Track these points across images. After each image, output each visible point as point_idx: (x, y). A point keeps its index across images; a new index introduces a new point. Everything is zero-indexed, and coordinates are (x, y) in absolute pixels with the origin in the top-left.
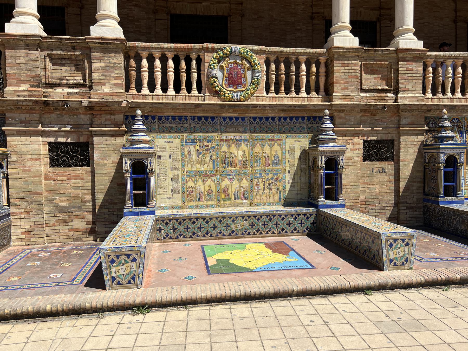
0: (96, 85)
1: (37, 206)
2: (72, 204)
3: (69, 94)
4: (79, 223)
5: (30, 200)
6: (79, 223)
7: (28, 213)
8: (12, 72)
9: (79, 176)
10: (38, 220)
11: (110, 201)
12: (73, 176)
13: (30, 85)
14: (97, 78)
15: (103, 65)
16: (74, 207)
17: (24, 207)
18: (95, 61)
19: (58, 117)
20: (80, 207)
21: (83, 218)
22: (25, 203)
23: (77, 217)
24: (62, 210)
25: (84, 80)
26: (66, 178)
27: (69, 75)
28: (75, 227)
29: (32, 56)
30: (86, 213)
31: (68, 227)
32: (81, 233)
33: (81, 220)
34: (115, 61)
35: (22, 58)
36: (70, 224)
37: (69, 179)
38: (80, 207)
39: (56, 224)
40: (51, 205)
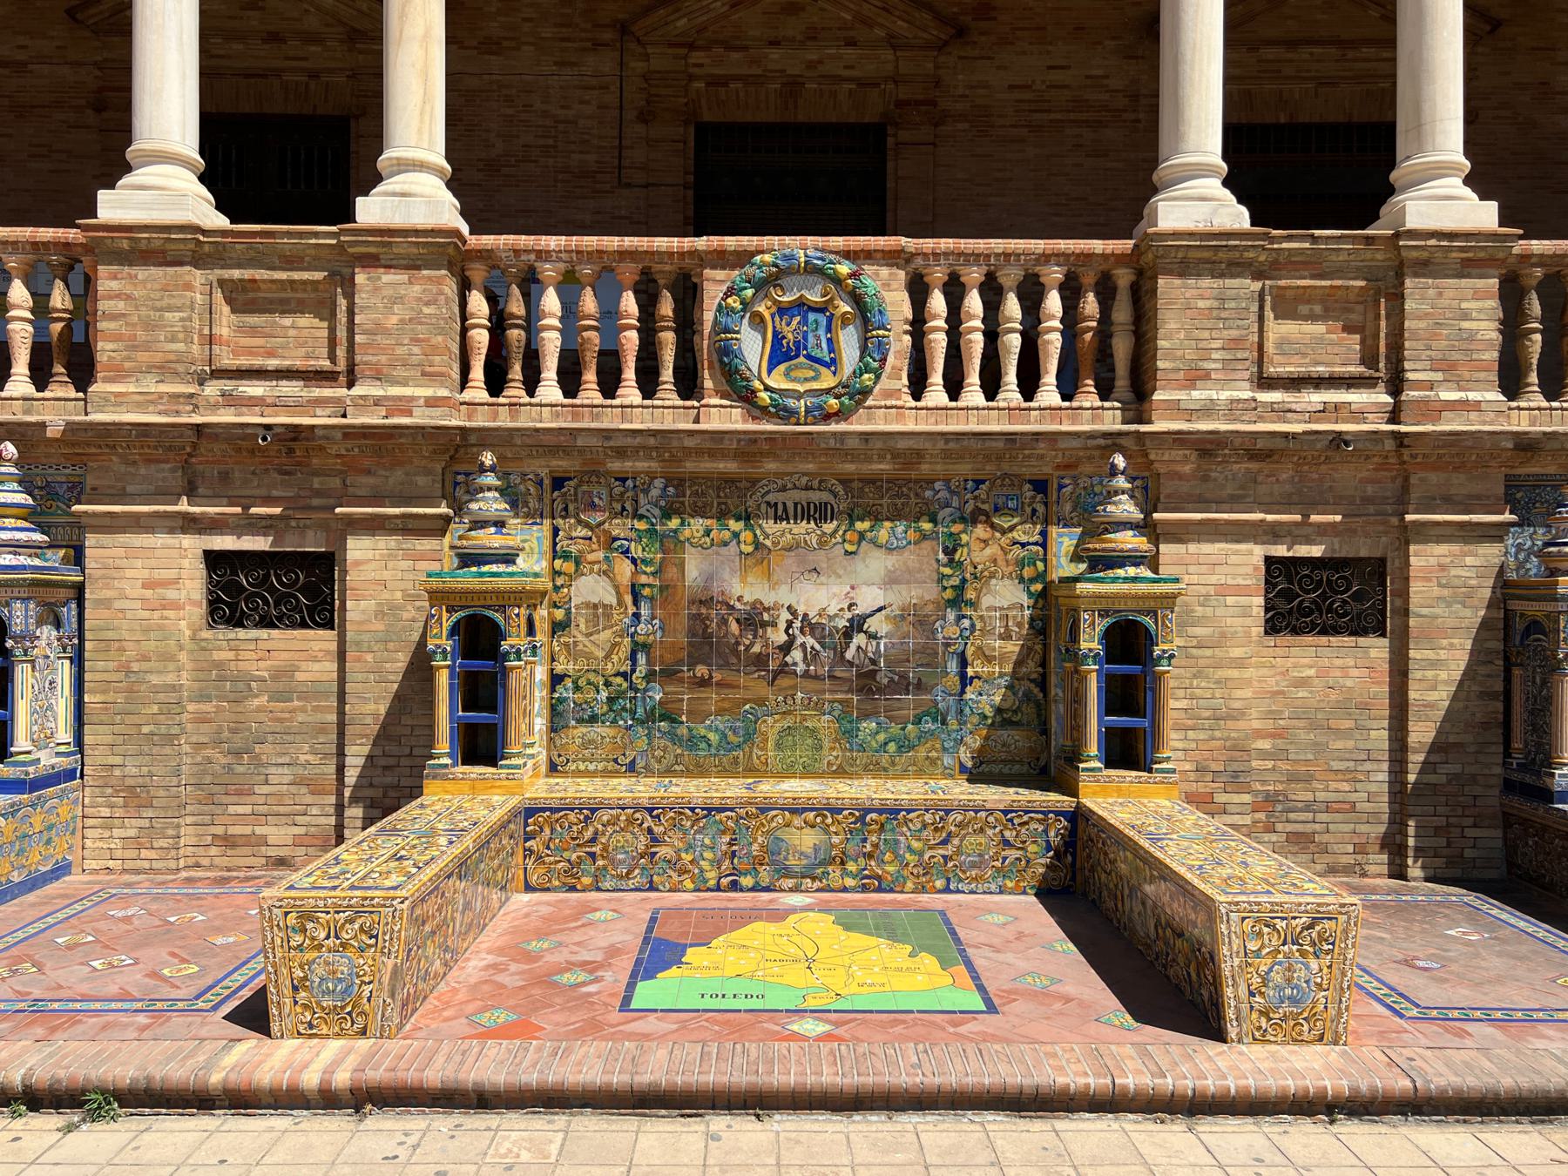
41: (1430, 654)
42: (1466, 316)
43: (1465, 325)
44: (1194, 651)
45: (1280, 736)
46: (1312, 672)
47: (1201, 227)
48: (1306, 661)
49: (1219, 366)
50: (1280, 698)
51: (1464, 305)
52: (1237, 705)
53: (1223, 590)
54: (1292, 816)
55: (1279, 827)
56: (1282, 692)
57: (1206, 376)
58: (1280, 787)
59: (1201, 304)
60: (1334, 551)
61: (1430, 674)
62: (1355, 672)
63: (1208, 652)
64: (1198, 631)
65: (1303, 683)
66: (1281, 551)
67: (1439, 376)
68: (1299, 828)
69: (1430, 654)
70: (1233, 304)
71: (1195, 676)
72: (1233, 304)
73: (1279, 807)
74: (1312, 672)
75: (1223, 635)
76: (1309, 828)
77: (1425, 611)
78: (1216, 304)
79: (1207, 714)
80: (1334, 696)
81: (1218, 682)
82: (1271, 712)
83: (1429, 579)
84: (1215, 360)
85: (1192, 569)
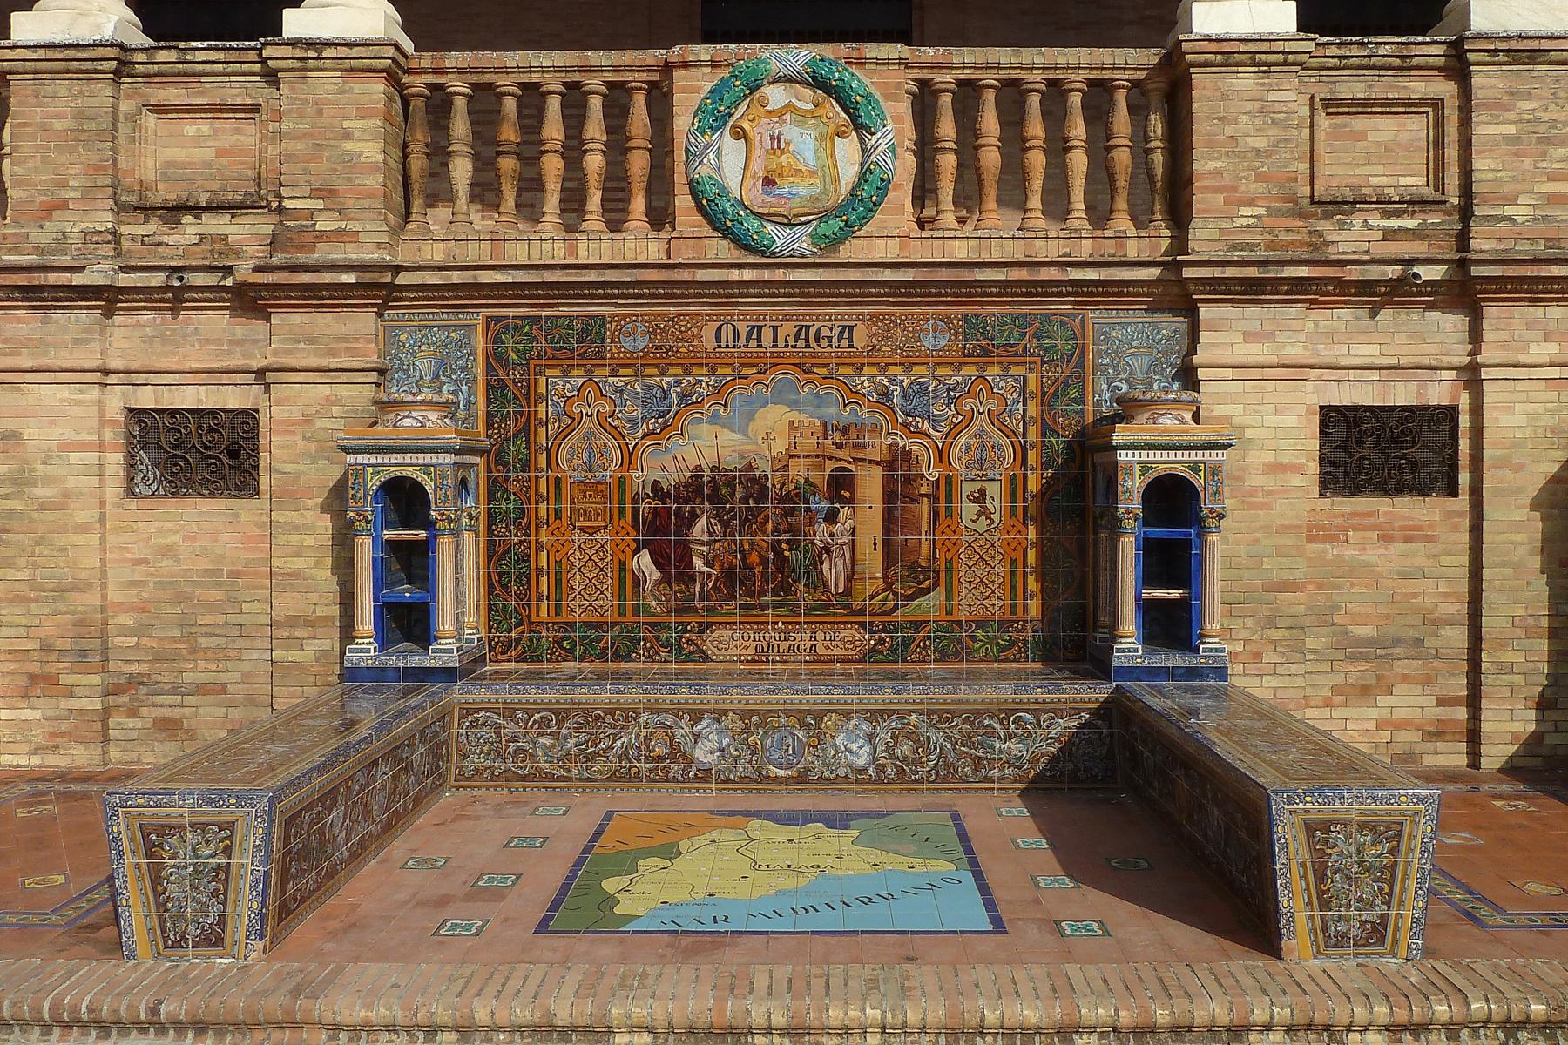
0: (1485, 202)
1: (1287, 633)
2: (1392, 631)
3: (1389, 235)
4: (1413, 701)
5: (1265, 612)
6: (1413, 701)
7: (1257, 656)
8: (1212, 165)
9: (1420, 528)
10: (1287, 681)
11: (1531, 621)
12: (1402, 528)
13: (1268, 208)
14: (1490, 176)
15: (1511, 129)
16: (1397, 641)
17: (1244, 634)
18: (1484, 118)
19: (1358, 319)
20: (1418, 642)
21: (1428, 680)
22: (1249, 622)
23: (1405, 679)
24: (1353, 649)
25: (1440, 186)
26: (1374, 535)
27: (1380, 169)
28: (1401, 714)
29: (1277, 107)
30: (1437, 664)
31: (1373, 713)
32: (1414, 736)
33: (1418, 690)
34: (1554, 116)
35: (1243, 119)
36: (1383, 700)
37: (1386, 538)
38: (1418, 642)
39: (1339, 699)
40: (1323, 631)
41: (294, 516)
42: (347, 135)
43: (348, 146)
44: (35, 515)
45: (142, 610)
46: (176, 538)
47: (58, 38)
48: (169, 525)
49: (78, 194)
50: (143, 567)
51: (346, 124)
52: (83, 575)
53: (67, 446)
54: (158, 699)
55: (144, 711)
56: (145, 561)
57: (63, 205)
58: (145, 667)
59: (58, 125)
60: (199, 401)
61: (295, 538)
62: (225, 537)
63: (49, 516)
64: (40, 491)
65: (167, 550)
66: (146, 398)
67: (319, 204)
68: (167, 712)
69: (294, 516)
70: (93, 126)
71: (37, 543)
72: (93, 126)
73: (144, 690)
74: (176, 538)
75: (66, 495)
76: (176, 713)
77: (289, 468)
78: (74, 125)
79: (51, 586)
80: (205, 564)
81: (63, 549)
82: (133, 583)
83: (293, 433)
84: (74, 189)
85: (32, 422)
